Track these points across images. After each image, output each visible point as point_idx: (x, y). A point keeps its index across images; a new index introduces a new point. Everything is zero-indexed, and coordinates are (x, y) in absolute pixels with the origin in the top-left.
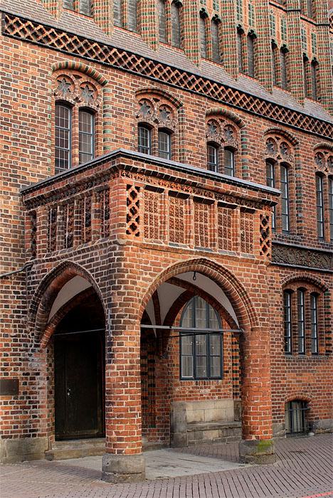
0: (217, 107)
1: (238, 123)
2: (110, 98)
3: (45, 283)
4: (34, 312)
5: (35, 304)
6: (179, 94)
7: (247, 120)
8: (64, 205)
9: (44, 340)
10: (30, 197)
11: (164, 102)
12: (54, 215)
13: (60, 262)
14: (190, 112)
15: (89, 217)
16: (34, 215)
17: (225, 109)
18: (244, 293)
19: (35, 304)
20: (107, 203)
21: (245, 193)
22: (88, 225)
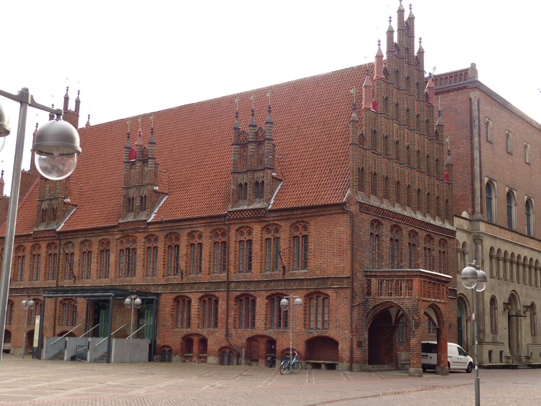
0: (411, 228)
1: (417, 233)
2: (384, 230)
3: (375, 307)
4: (367, 316)
5: (368, 313)
6: (402, 226)
7: (420, 232)
8: (387, 281)
9: (368, 326)
10: (369, 274)
11: (397, 228)
12: (382, 283)
13: (385, 301)
14: (405, 233)
15: (401, 288)
16: (370, 280)
17: (414, 228)
18: (441, 314)
19: (368, 313)
20: (411, 285)
21: (444, 279)
22: (401, 290)
